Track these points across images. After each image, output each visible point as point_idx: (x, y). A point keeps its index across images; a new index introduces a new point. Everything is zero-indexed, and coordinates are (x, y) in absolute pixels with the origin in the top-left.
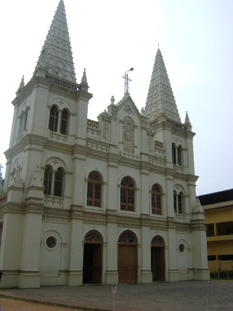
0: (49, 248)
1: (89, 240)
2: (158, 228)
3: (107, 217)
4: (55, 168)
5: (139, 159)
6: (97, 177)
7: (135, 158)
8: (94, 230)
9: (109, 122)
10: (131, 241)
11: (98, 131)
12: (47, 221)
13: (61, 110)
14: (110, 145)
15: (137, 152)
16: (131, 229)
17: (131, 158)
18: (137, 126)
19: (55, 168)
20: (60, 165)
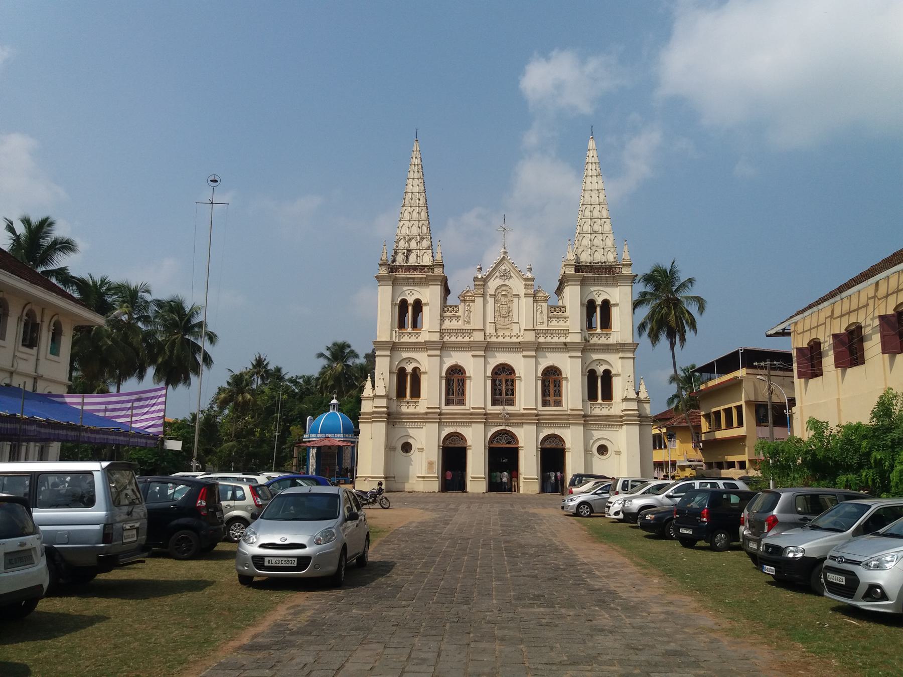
0: (405, 454)
1: (450, 443)
2: (551, 425)
3: (470, 418)
4: (409, 369)
5: (520, 339)
6: (460, 371)
7: (514, 340)
8: (456, 432)
9: (473, 301)
10: (509, 442)
11: (458, 317)
12: (399, 426)
13: (411, 304)
14: (474, 330)
15: (515, 329)
16: (507, 428)
17: (507, 340)
18: (517, 296)
19: (409, 369)
20: (414, 365)
